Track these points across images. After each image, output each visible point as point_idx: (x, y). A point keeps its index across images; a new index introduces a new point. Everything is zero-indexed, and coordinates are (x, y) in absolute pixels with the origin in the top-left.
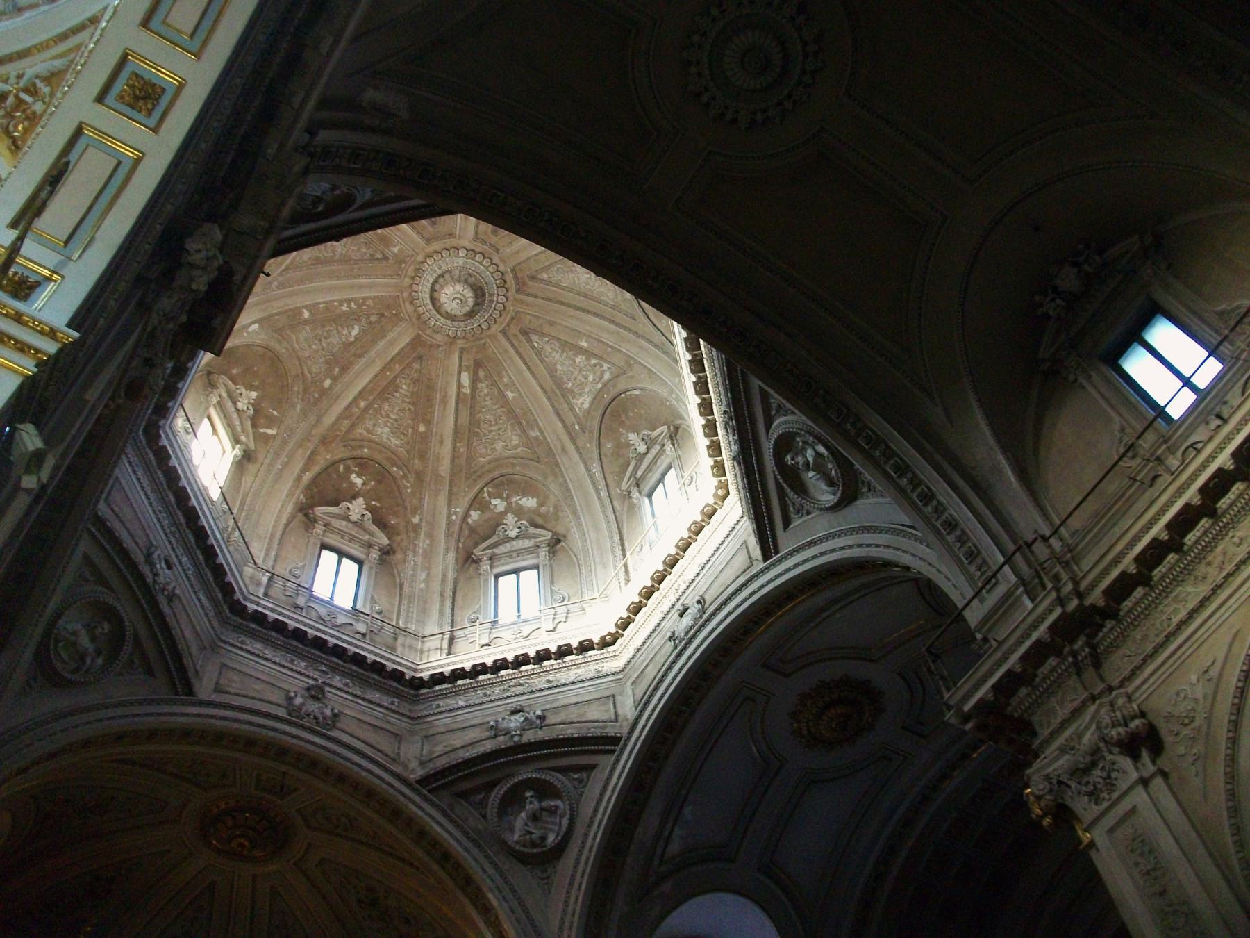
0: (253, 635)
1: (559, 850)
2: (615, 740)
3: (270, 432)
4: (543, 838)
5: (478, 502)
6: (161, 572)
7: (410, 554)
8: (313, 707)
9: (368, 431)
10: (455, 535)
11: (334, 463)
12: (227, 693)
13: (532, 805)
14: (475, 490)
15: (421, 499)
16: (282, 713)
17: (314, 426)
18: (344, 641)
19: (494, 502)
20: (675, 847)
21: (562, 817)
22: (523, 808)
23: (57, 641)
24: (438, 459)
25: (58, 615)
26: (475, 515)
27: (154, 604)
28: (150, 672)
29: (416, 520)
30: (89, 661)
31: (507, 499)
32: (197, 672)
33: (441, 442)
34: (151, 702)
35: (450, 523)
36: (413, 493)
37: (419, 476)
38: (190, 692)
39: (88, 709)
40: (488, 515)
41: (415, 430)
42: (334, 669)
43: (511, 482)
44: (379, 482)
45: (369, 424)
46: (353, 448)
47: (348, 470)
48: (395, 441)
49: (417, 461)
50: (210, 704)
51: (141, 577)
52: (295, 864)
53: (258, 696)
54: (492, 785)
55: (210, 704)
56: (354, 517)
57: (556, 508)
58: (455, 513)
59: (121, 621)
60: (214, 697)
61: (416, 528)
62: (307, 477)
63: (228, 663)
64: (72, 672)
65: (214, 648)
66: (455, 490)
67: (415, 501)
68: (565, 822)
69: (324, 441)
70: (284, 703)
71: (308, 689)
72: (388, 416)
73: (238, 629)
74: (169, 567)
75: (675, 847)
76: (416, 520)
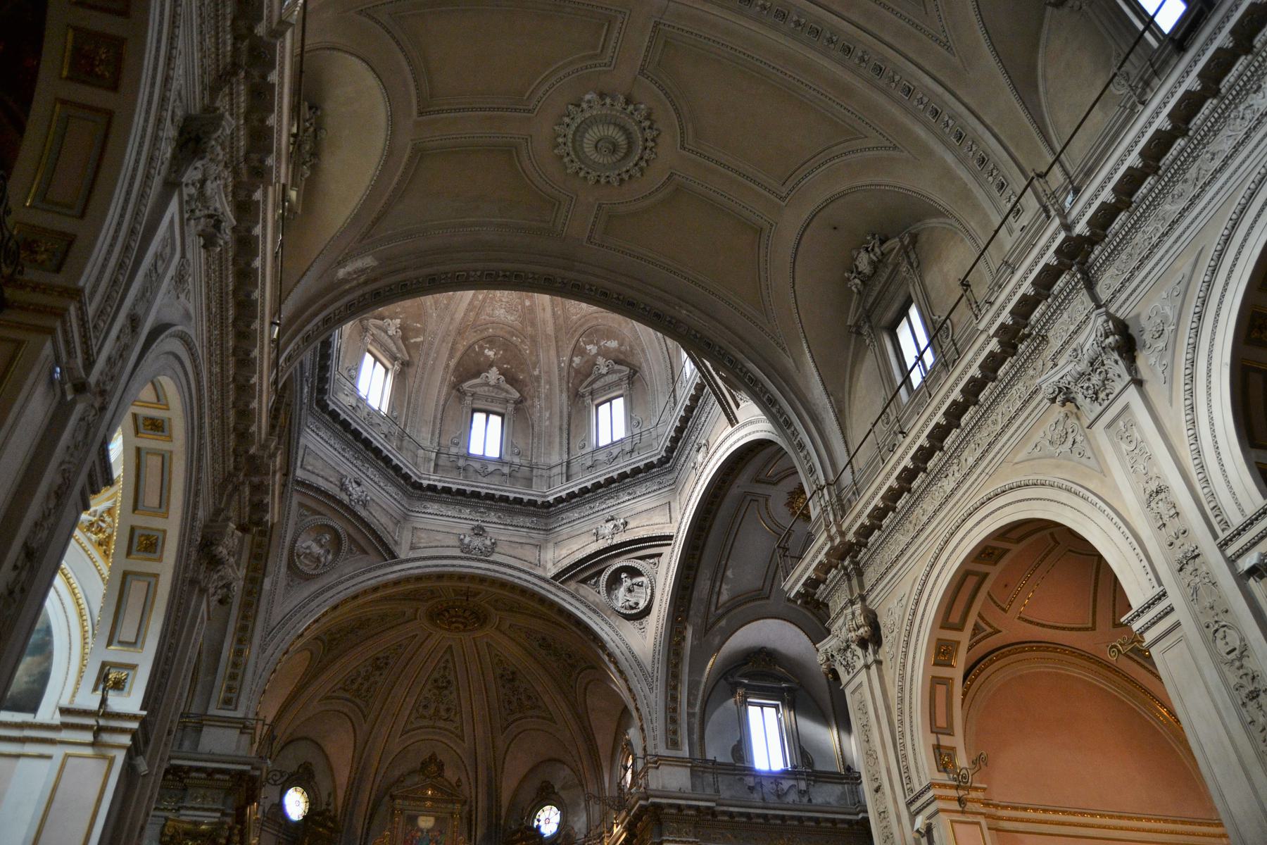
0: (432, 500)
1: (647, 611)
2: (670, 537)
3: (418, 340)
4: (637, 604)
5: (578, 350)
6: (353, 492)
7: (536, 400)
8: (477, 542)
9: (488, 315)
10: (566, 379)
11: (471, 347)
12: (419, 548)
13: (627, 582)
14: (574, 342)
15: (537, 356)
16: (457, 552)
17: (450, 323)
18: (492, 489)
19: (589, 347)
20: (725, 597)
21: (647, 588)
22: (621, 583)
23: (299, 556)
24: (544, 322)
25: (294, 541)
26: (577, 360)
27: (355, 514)
28: (364, 552)
29: (536, 373)
30: (323, 559)
31: (597, 344)
32: (396, 542)
33: (544, 309)
34: (370, 571)
35: (560, 369)
36: (531, 352)
37: (534, 340)
38: (393, 555)
39: (330, 588)
40: (585, 359)
41: (523, 304)
42: (489, 509)
43: (597, 331)
44: (505, 350)
45: (488, 310)
46: (482, 331)
47: (482, 348)
48: (510, 318)
49: (529, 328)
50: (408, 561)
51: (340, 502)
52: (497, 628)
53: (439, 544)
54: (600, 573)
55: (408, 561)
56: (492, 383)
57: (630, 347)
58: (563, 361)
59: (336, 531)
60: (412, 555)
61: (538, 379)
62: (453, 363)
63: (418, 526)
64: (315, 569)
65: (406, 517)
66: (560, 343)
67: (534, 358)
68: (649, 591)
69: (460, 333)
70: (458, 544)
71: (473, 529)
72: (501, 301)
73: (420, 498)
74: (359, 484)
75: (725, 597)
76: (536, 373)
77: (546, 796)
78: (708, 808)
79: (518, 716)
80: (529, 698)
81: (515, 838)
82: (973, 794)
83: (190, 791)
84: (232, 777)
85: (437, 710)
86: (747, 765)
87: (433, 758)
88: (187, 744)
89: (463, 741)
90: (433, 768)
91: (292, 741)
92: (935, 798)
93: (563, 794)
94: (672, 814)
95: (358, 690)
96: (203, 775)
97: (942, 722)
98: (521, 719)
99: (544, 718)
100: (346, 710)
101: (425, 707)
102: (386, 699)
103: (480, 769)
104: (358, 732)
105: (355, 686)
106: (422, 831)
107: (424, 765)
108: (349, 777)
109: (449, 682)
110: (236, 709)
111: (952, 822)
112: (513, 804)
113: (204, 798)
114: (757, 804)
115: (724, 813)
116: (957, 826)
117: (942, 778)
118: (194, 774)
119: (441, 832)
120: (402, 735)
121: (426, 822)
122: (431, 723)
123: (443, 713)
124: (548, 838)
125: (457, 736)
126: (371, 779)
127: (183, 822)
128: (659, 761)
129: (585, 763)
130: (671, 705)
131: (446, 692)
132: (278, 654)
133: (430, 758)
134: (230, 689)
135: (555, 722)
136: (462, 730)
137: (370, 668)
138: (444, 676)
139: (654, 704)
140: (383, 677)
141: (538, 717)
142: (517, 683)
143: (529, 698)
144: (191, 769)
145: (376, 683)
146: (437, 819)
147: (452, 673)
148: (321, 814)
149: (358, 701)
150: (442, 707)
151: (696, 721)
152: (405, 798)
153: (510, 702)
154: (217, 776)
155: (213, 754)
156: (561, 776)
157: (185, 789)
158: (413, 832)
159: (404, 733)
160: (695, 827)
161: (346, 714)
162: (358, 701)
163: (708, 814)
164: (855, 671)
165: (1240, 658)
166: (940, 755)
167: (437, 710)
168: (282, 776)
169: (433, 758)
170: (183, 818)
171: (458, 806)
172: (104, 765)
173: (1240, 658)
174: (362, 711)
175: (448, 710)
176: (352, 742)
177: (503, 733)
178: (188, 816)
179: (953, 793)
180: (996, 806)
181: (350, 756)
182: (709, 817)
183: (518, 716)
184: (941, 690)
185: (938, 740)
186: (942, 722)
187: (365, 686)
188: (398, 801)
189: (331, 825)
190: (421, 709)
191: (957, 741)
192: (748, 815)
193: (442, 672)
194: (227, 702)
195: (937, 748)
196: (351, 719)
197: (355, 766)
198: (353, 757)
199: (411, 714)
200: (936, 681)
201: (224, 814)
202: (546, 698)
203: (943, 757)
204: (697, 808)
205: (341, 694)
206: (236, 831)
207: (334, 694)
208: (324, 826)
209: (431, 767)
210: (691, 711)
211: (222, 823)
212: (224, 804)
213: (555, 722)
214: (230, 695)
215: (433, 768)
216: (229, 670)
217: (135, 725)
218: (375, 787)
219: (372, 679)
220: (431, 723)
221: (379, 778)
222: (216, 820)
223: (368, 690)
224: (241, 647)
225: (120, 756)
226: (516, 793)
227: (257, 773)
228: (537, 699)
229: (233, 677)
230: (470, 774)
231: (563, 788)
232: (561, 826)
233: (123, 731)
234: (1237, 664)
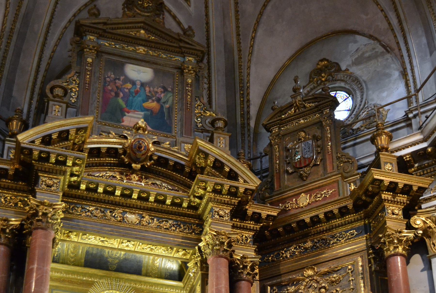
106: (133, 83)
158: (119, 83)
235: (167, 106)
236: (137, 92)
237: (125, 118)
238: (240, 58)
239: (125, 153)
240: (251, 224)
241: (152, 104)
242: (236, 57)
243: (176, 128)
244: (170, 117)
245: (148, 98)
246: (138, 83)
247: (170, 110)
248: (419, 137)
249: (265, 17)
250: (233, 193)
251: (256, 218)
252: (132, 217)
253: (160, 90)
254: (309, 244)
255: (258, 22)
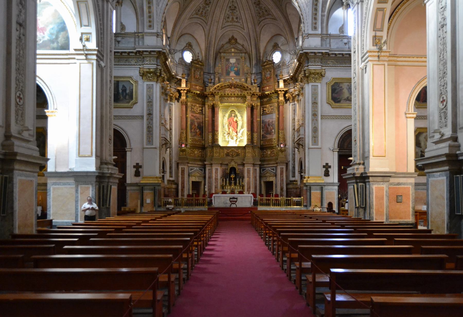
77: (276, 48)
78: (326, 53)
79: (263, 18)
80: (266, 11)
81: (264, 64)
82: (383, 54)
83: (145, 59)
84: (157, 53)
85: (233, 18)
86: (345, 34)
87: (233, 37)
88: (140, 42)
89: (244, 30)
90: (233, 41)
91: (182, 36)
92: (370, 56)
93: (282, 47)
94: (312, 56)
95: (201, 14)
96: (148, 53)
97: (379, 26)
98: (264, 19)
99: (273, 19)
100: (199, 22)
101: (228, 18)
102: (213, 16)
103: (251, 40)
104: (205, 30)
105: (200, 13)
106: (232, 64)
107: (230, 41)
108: (205, 46)
109: (235, 7)
110: (153, 29)
111: (373, 64)
112: (265, 52)
113: (150, 61)
114: (346, 50)
115: (333, 54)
116: (375, 66)
117: (375, 48)
118: (145, 53)
119: (238, 64)
120: (221, 29)
121: (233, 61)
122: (231, 24)
123: (235, 19)
124: (277, 63)
125: (242, 28)
126: (213, 46)
127: (145, 69)
128: (309, 35)
129: (289, 35)
130: (314, 12)
131: (235, 11)
132: (164, 6)
133: (232, 37)
134: (150, 22)
135: (277, 20)
136: (243, 25)
137: (204, 5)
138: (233, 5)
139: (308, 12)
140: (210, 7)
141: (270, 18)
142: (261, 5)
143: (266, 11)
144: (143, 51)
145: (208, 10)
146: (237, 59)
147: (236, 3)
148: (196, 60)
149: (202, 18)
150: (235, 18)
151: (325, 18)
152: (225, 53)
153: (259, 13)
154: (152, 53)
155: (149, 46)
156: (281, 41)
157: (143, 58)
158: (229, 64)
159: (222, 28)
160: (321, 60)
161: (199, 24)
162: (202, 18)
163: (326, 55)
164: (355, 5)
165: (443, 11)
166: (375, 39)
167: (233, 18)
168: (174, 51)
169: (233, 37)
170: (145, 67)
171: (243, 54)
172: (91, 65)
173: (443, 11)
174: (205, 22)
175: (237, 18)
176: (204, 33)
177: (258, 25)
178: (146, 67)
179: (376, 54)
180: (398, 57)
181: (204, 38)
182: (327, 56)
183: (263, 18)
184: (380, 13)
185: (376, 34)
186: (379, 26)
187: (204, 11)
188: (222, 54)
189: (201, 64)
190: (227, 19)
191: (384, 34)
192: (342, 54)
193: (232, 4)
194: (150, 26)
195: (375, 37)
196: (201, 25)
197: (206, 43)
198: (205, 39)
199: (223, 20)
200: (379, 9)
201: (157, 65)
202: (273, 11)
203: (376, 40)
204: (322, 53)
205: (196, 16)
206: (162, 71)
207: (193, 16)
208: (198, 64)
209: (233, 40)
210: (323, 14)
211: (157, 68)
212: (157, 62)
213: (277, 20)
214: (150, 24)
215: (233, 41)
216: (148, 15)
217: (96, 52)
218: (215, 49)
219: (206, 9)
220: (231, 24)
221: (216, 46)
222: (155, 67)
223: (205, 13)
224: (150, 5)
225: (95, 62)
226: (266, 47)
227: (165, 51)
228: (269, 11)
229: (150, 17)
230: (248, 43)
231: (282, 45)
232: (282, 58)
233: (93, 54)
234: (442, 13)
235: (239, 68)
236: (232, 66)
237: (231, 74)
238: (258, 42)
239: (230, 85)
240: (256, 96)
241: (236, 69)
242: (257, 41)
243: (241, 74)
244: (239, 71)
245: (235, 67)
246: (233, 64)
247: (239, 69)
248: (288, 75)
249: (262, 32)
250: (251, 93)
251: (257, 95)
252: (233, 99)
253: (237, 64)
254: (268, 99)
255: (260, 33)
